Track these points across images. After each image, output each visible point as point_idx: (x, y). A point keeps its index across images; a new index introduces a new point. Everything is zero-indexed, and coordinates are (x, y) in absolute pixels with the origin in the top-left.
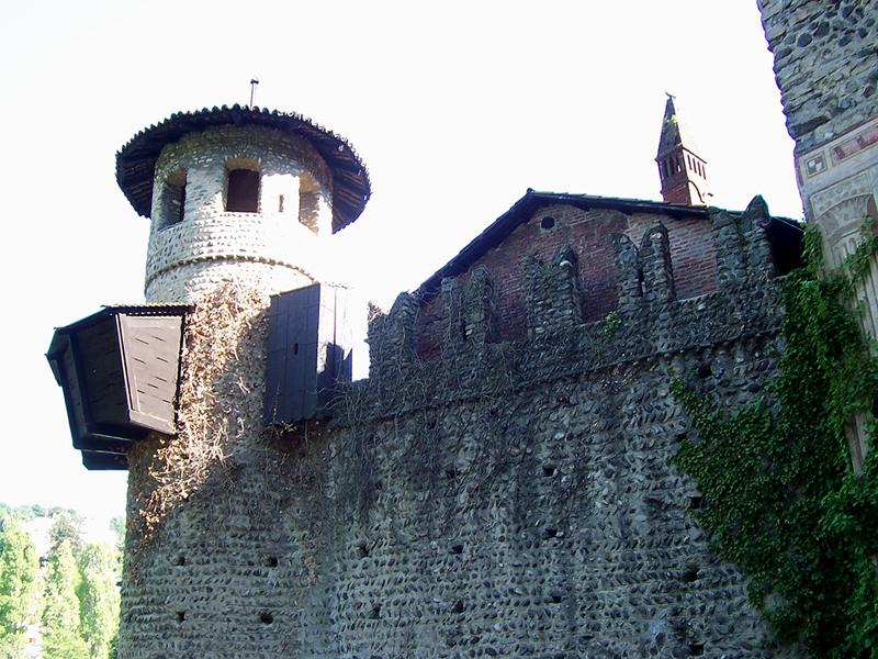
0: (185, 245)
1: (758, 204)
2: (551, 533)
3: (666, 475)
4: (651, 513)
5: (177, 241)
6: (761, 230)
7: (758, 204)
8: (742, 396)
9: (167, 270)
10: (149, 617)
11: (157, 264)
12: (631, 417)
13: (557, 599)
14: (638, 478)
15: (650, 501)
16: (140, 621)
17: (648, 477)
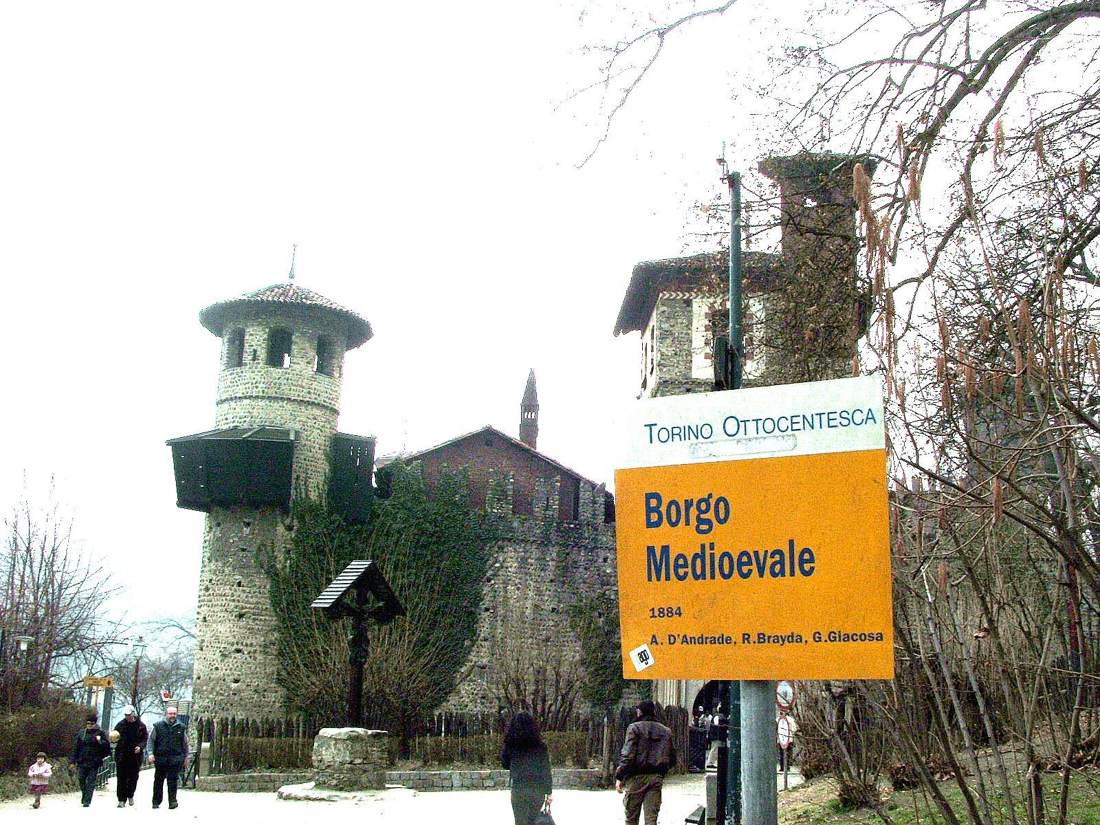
0: (293, 388)
1: (603, 485)
2: (487, 610)
3: (544, 595)
4: (534, 610)
5: (285, 381)
6: (604, 500)
7: (603, 485)
8: (581, 570)
9: (275, 399)
10: (263, 618)
11: (266, 390)
12: (532, 565)
13: (486, 640)
14: (531, 594)
15: (536, 606)
16: (254, 619)
17: (536, 595)
